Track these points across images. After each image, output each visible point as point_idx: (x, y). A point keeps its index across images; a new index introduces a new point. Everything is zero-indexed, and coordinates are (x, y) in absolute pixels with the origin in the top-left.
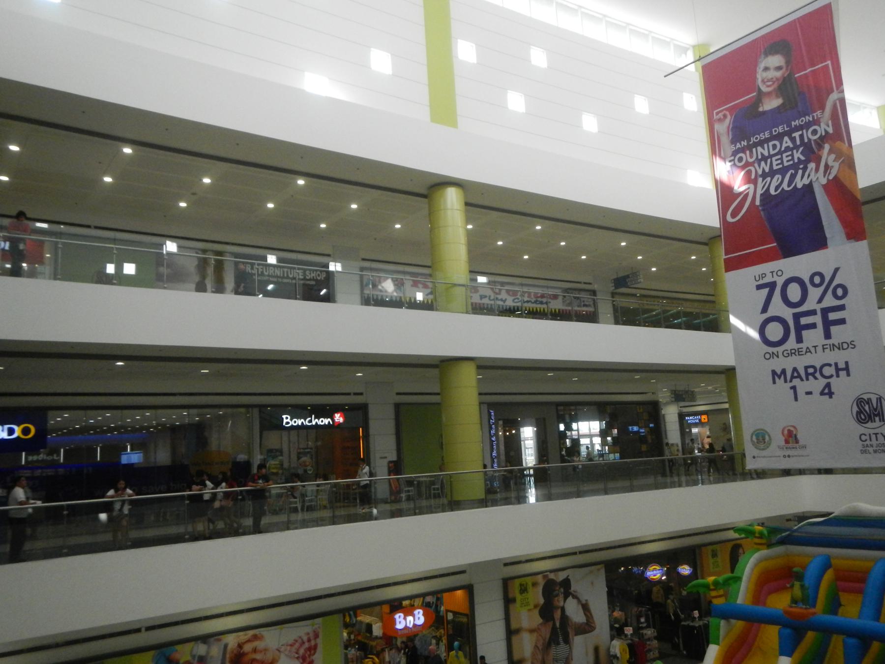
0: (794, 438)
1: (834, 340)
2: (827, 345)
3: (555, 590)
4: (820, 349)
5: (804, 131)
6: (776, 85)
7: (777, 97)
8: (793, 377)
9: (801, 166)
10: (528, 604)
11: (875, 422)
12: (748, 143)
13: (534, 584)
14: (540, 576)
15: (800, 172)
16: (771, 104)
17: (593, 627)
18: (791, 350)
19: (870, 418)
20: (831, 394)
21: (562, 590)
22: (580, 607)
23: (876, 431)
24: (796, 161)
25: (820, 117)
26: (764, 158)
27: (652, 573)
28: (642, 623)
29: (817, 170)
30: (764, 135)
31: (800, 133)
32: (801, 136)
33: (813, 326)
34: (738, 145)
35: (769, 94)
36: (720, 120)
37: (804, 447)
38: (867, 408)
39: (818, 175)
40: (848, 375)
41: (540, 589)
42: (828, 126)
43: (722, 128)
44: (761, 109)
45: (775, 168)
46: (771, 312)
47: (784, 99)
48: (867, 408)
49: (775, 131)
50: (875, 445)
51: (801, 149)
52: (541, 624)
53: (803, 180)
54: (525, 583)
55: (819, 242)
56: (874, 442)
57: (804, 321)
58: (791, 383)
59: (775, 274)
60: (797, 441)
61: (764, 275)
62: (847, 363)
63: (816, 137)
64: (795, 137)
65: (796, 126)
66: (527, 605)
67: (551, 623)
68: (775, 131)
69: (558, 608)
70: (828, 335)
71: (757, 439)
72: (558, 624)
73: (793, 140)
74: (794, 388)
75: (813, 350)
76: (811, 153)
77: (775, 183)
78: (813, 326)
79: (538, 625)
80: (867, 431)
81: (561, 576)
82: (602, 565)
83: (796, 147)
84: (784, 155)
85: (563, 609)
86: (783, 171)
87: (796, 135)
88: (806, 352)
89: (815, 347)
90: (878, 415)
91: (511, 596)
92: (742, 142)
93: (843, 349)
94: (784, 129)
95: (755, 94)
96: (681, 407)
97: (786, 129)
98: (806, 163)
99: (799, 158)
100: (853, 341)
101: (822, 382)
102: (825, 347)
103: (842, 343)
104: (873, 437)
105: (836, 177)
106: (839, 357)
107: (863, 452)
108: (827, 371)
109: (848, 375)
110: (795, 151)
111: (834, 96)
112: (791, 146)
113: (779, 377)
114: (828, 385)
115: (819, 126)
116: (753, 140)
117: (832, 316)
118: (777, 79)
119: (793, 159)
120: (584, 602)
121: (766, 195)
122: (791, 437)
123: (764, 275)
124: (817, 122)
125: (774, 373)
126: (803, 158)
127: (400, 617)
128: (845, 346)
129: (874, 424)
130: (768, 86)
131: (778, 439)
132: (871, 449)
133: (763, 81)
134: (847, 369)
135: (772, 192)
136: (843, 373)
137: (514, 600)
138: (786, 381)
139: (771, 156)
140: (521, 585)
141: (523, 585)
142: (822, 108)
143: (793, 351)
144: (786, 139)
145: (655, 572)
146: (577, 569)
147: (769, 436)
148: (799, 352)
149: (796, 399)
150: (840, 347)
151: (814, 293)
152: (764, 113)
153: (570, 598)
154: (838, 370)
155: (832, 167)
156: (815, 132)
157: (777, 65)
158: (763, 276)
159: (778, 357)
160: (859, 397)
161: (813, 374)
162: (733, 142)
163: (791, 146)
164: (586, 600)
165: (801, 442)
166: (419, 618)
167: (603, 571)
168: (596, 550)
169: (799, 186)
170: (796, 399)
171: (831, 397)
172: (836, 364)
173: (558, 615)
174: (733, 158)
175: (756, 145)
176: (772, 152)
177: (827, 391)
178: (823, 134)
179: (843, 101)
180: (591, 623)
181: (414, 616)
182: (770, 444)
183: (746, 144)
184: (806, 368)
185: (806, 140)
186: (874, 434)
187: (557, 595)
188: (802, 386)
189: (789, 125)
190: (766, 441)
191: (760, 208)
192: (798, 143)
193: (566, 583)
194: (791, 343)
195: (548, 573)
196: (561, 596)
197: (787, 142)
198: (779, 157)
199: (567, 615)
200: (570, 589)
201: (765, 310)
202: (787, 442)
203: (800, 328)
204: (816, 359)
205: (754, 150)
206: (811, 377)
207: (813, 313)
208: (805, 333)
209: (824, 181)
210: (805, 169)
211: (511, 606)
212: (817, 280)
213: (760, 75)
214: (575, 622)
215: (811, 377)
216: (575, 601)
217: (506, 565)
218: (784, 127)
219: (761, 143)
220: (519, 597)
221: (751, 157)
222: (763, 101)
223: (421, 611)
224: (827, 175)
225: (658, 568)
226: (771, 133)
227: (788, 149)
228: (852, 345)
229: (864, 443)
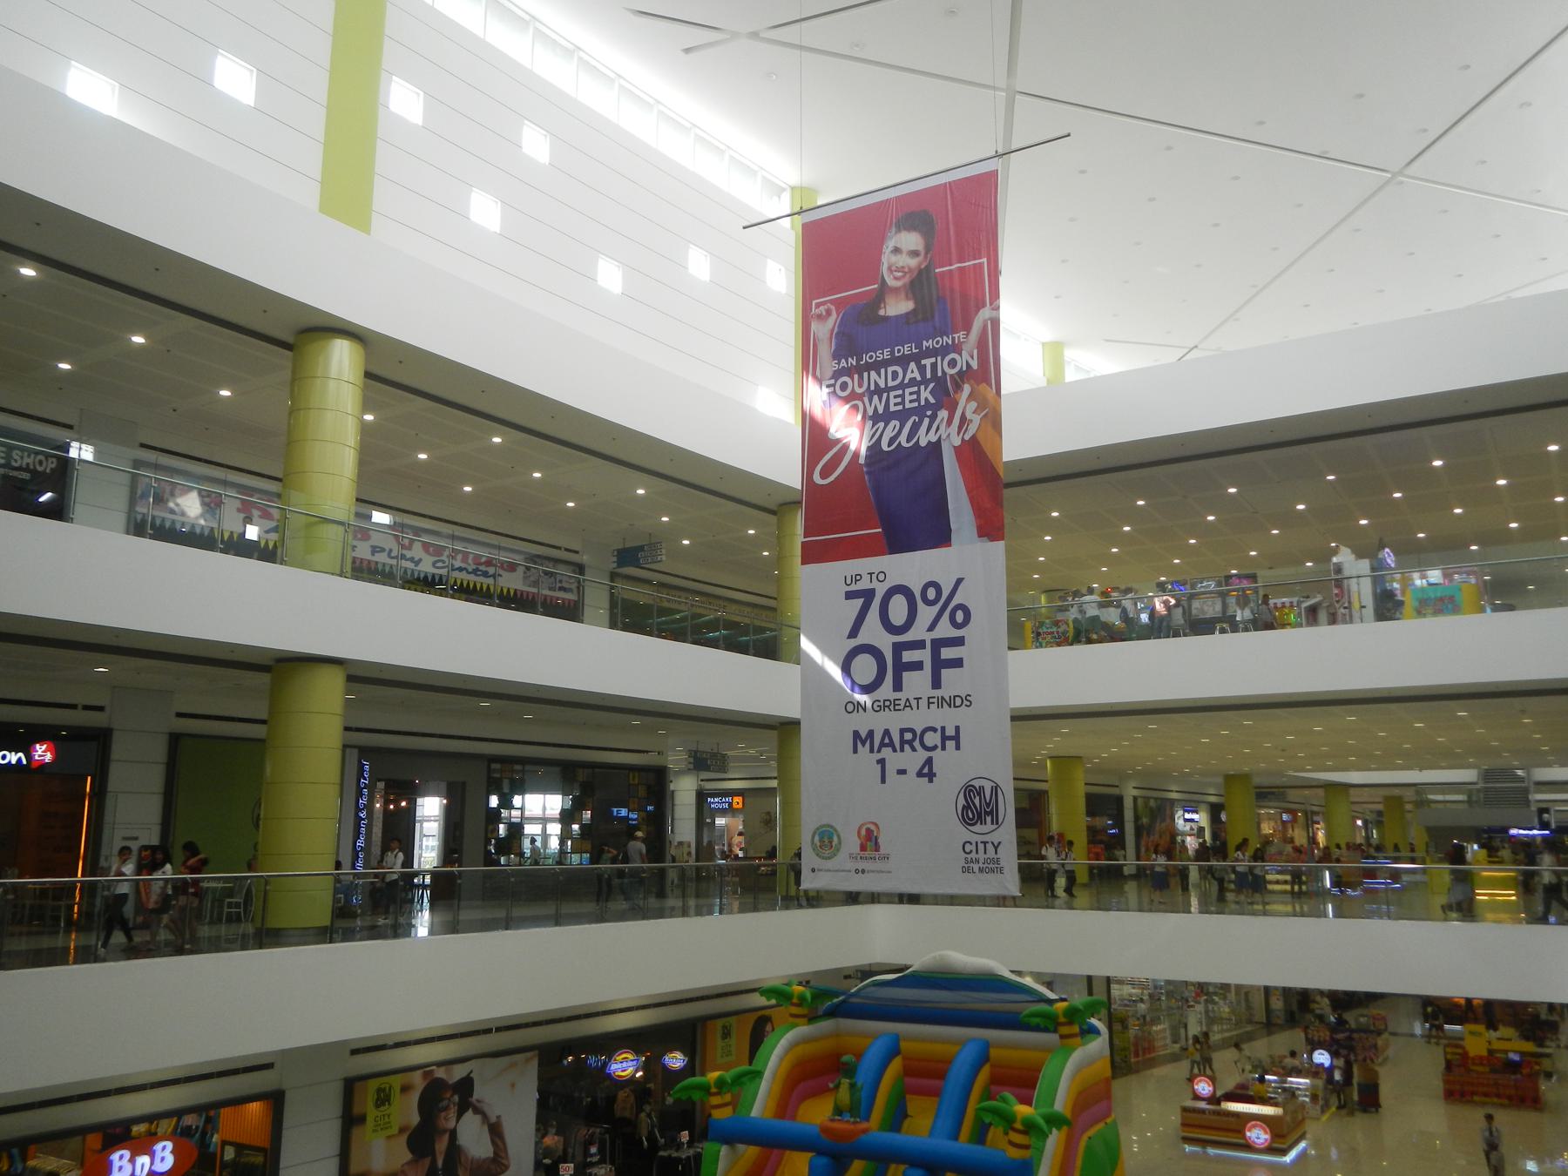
0: (873, 843)
1: (945, 692)
2: (934, 697)
3: (442, 1100)
4: (923, 703)
5: (939, 358)
6: (907, 279)
7: (907, 298)
8: (882, 745)
9: (929, 413)
10: (387, 1126)
11: (985, 823)
12: (857, 362)
13: (405, 1089)
14: (419, 1073)
15: (926, 421)
16: (897, 307)
17: (503, 1164)
18: (885, 701)
19: (979, 818)
20: (931, 776)
21: (456, 1098)
22: (486, 1128)
23: (985, 838)
24: (923, 403)
25: (964, 342)
26: (879, 391)
27: (619, 1066)
28: (592, 1156)
29: (949, 422)
30: (883, 353)
31: (933, 360)
32: (934, 366)
33: (918, 666)
34: (843, 363)
35: (896, 290)
36: (819, 317)
37: (886, 857)
38: (977, 801)
39: (949, 431)
40: (958, 748)
41: (415, 1097)
42: (973, 358)
43: (823, 330)
44: (882, 312)
45: (893, 408)
46: (862, 639)
47: (916, 303)
48: (977, 801)
49: (899, 351)
50: (982, 861)
51: (932, 385)
52: (408, 1163)
53: (929, 434)
54: (388, 1086)
55: (940, 536)
56: (981, 856)
57: (908, 656)
58: (879, 754)
59: (874, 576)
60: (877, 848)
61: (858, 578)
62: (957, 728)
63: (953, 371)
64: (925, 365)
65: (927, 348)
66: (387, 1128)
67: (427, 1161)
68: (899, 351)
69: (445, 1131)
70: (936, 683)
71: (821, 840)
72: (440, 1163)
73: (922, 369)
74: (882, 762)
75: (914, 703)
76: (945, 395)
77: (889, 434)
78: (918, 666)
79: (403, 1166)
80: (973, 838)
81: (459, 1072)
82: (537, 1052)
83: (925, 382)
84: (908, 391)
85: (453, 1134)
86: (902, 416)
87: (927, 362)
88: (905, 706)
89: (918, 699)
90: (991, 813)
91: (357, 1110)
92: (850, 359)
93: (955, 706)
94: (911, 350)
95: (876, 286)
96: (702, 780)
97: (914, 351)
98: (936, 408)
99: (926, 399)
100: (970, 696)
101: (922, 755)
102: (931, 700)
103: (954, 697)
104: (981, 847)
105: (974, 438)
106: (947, 718)
107: (966, 870)
108: (932, 739)
109: (958, 748)
110: (922, 387)
111: (985, 313)
112: (919, 378)
113: (863, 744)
114: (929, 761)
115: (961, 355)
116: (866, 358)
117: (947, 653)
118: (910, 270)
119: (918, 400)
120: (493, 1120)
122: (870, 840)
123: (858, 578)
124: (957, 348)
125: (856, 734)
126: (932, 400)
127: (121, 1157)
128: (958, 702)
129: (983, 826)
130: (896, 278)
131: (852, 843)
132: (976, 867)
133: (890, 269)
134: (956, 738)
135: (885, 447)
136: (950, 744)
137: (362, 1119)
138: (872, 751)
139: (888, 389)
140: (379, 1090)
141: (384, 1090)
142: (967, 328)
143: (887, 703)
144: (913, 365)
145: (624, 1065)
146: (487, 1060)
147: (839, 837)
148: (895, 705)
149: (883, 780)
150: (951, 703)
151: (926, 614)
152: (886, 319)
153: (469, 1116)
154: (944, 738)
155: (971, 421)
156: (953, 363)
157: (913, 248)
158: (857, 578)
159: (865, 710)
160: (970, 783)
161: (910, 743)
162: (837, 356)
163: (919, 378)
164: (499, 1117)
165: (883, 851)
166: (163, 1159)
167: (535, 1063)
168: (527, 1025)
169: (923, 443)
170: (883, 780)
171: (931, 781)
172: (943, 729)
173: (441, 1145)
174: (832, 381)
175: (869, 367)
176: (891, 384)
177: (927, 772)
178: (964, 368)
179: (996, 323)
180: (503, 1158)
181: (152, 1155)
182: (838, 850)
183: (854, 363)
184: (902, 731)
185: (940, 374)
186: (982, 842)
187: (446, 1108)
188: (894, 760)
189: (919, 346)
190: (834, 844)
191: (865, 469)
192: (929, 376)
193: (466, 1085)
194: (886, 690)
195: (434, 1067)
196: (453, 1111)
197: (913, 372)
198: (900, 392)
199: (459, 1146)
200: (471, 1096)
201: (854, 633)
202: (863, 848)
203: (901, 668)
204: (916, 719)
205: (866, 374)
206: (907, 747)
207: (919, 645)
208: (906, 675)
209: (957, 442)
210: (933, 418)
211: (356, 1132)
212: (931, 594)
213: (887, 259)
214: (473, 1159)
215: (907, 747)
216: (478, 1118)
217: (355, 1052)
218: (911, 347)
219: (877, 366)
220: (372, 1113)
221: (860, 386)
222: (887, 300)
223: (169, 1145)
224: (962, 434)
225: (630, 1057)
226: (892, 352)
227: (913, 382)
228: (967, 701)
229: (967, 856)
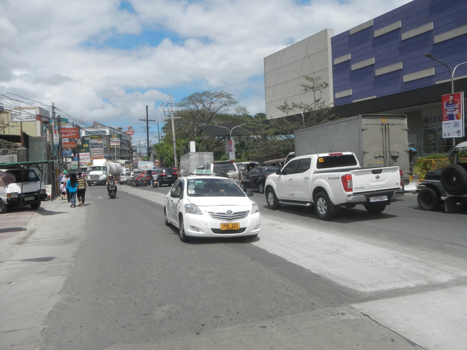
16: (451, 103)
86: (452, 111)
121: (449, 114)
124: (456, 106)
213: (450, 99)
219: (450, 107)
